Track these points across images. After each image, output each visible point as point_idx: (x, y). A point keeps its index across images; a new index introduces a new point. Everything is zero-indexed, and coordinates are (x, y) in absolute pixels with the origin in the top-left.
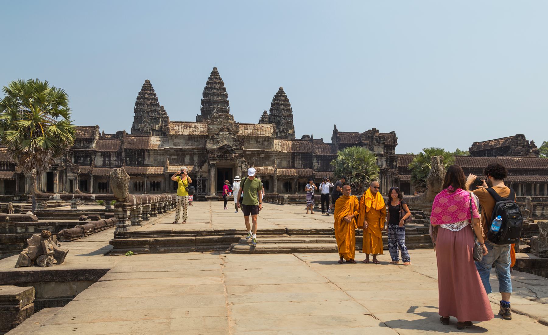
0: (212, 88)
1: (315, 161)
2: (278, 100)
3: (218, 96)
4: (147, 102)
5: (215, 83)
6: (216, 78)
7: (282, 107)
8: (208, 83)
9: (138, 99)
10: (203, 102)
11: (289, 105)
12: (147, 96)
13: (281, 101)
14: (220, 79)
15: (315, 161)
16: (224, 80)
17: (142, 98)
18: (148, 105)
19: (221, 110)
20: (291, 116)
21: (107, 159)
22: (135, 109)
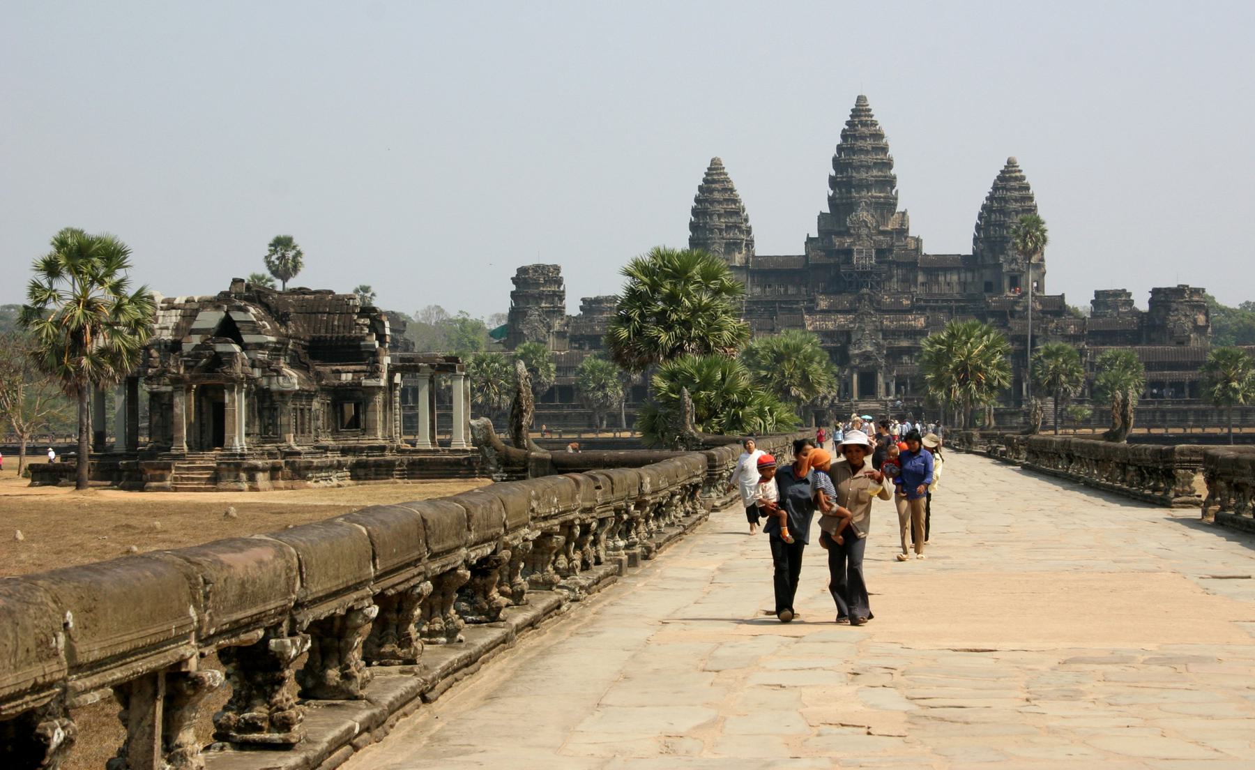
2: (1004, 188)
3: (868, 168)
4: (718, 207)
5: (863, 138)
6: (864, 124)
7: (1014, 206)
8: (844, 136)
9: (697, 200)
10: (833, 182)
11: (1031, 199)
12: (717, 195)
14: (874, 124)
17: (706, 200)
18: (720, 216)
19: (876, 203)
22: (691, 223)
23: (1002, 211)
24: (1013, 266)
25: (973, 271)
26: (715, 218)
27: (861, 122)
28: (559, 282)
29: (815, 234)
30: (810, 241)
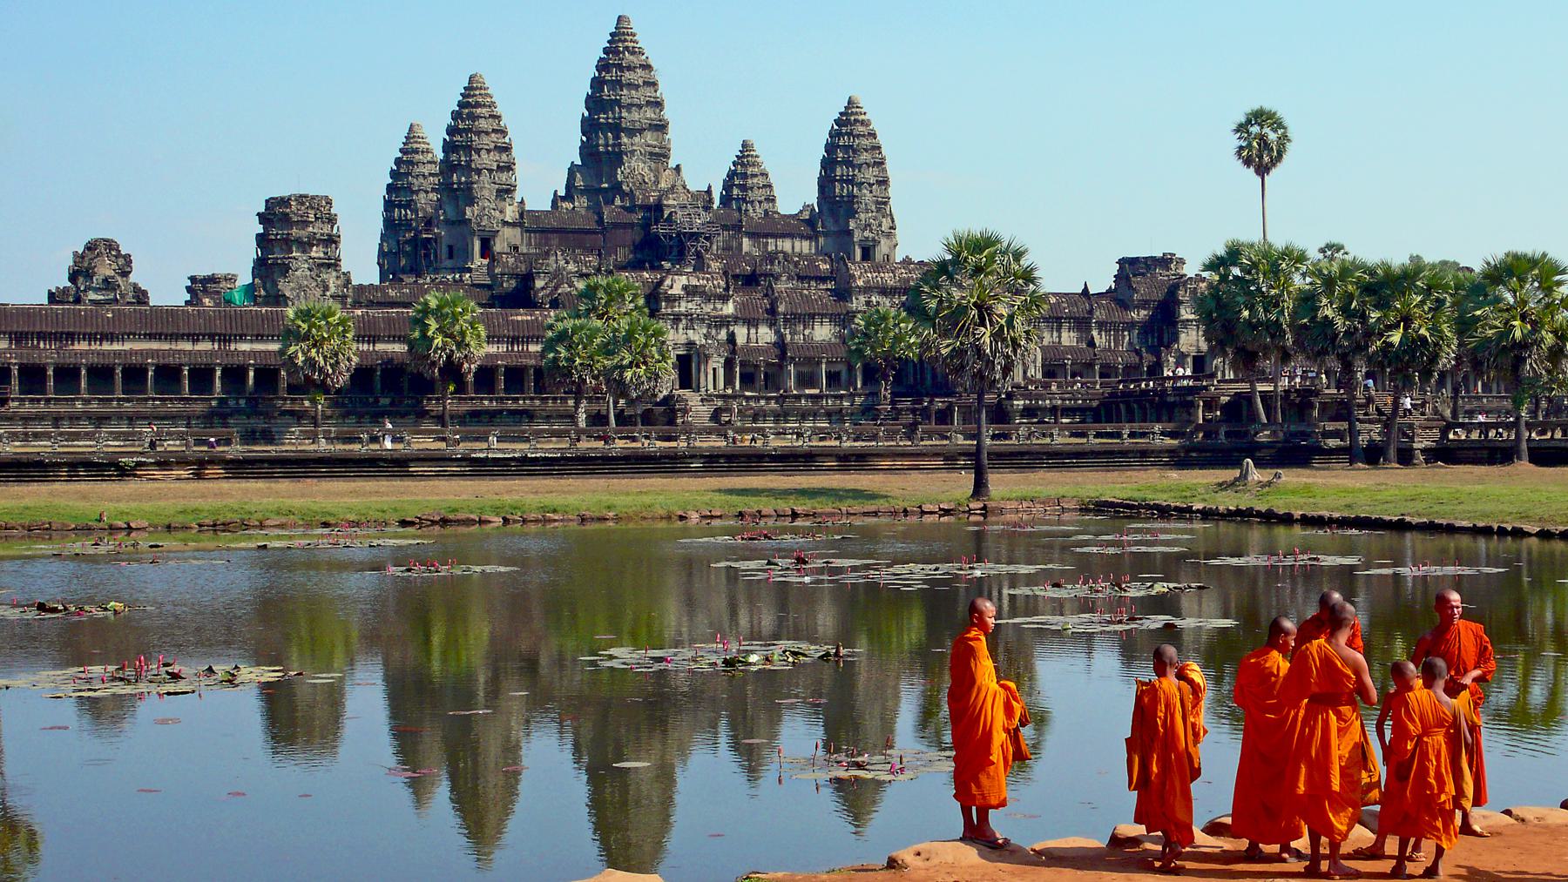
0: (618, 84)
1: (1095, 333)
2: (850, 134)
4: (485, 139)
5: (629, 68)
6: (633, 53)
7: (865, 157)
8: (603, 66)
12: (483, 124)
13: (858, 136)
15: (1095, 333)
16: (652, 54)
18: (489, 151)
19: (651, 154)
20: (884, 182)
21: (753, 331)
23: (848, 163)
24: (867, 234)
25: (809, 238)
26: (483, 153)
27: (627, 48)
28: (332, 220)
29: (562, 193)
30: (556, 200)
